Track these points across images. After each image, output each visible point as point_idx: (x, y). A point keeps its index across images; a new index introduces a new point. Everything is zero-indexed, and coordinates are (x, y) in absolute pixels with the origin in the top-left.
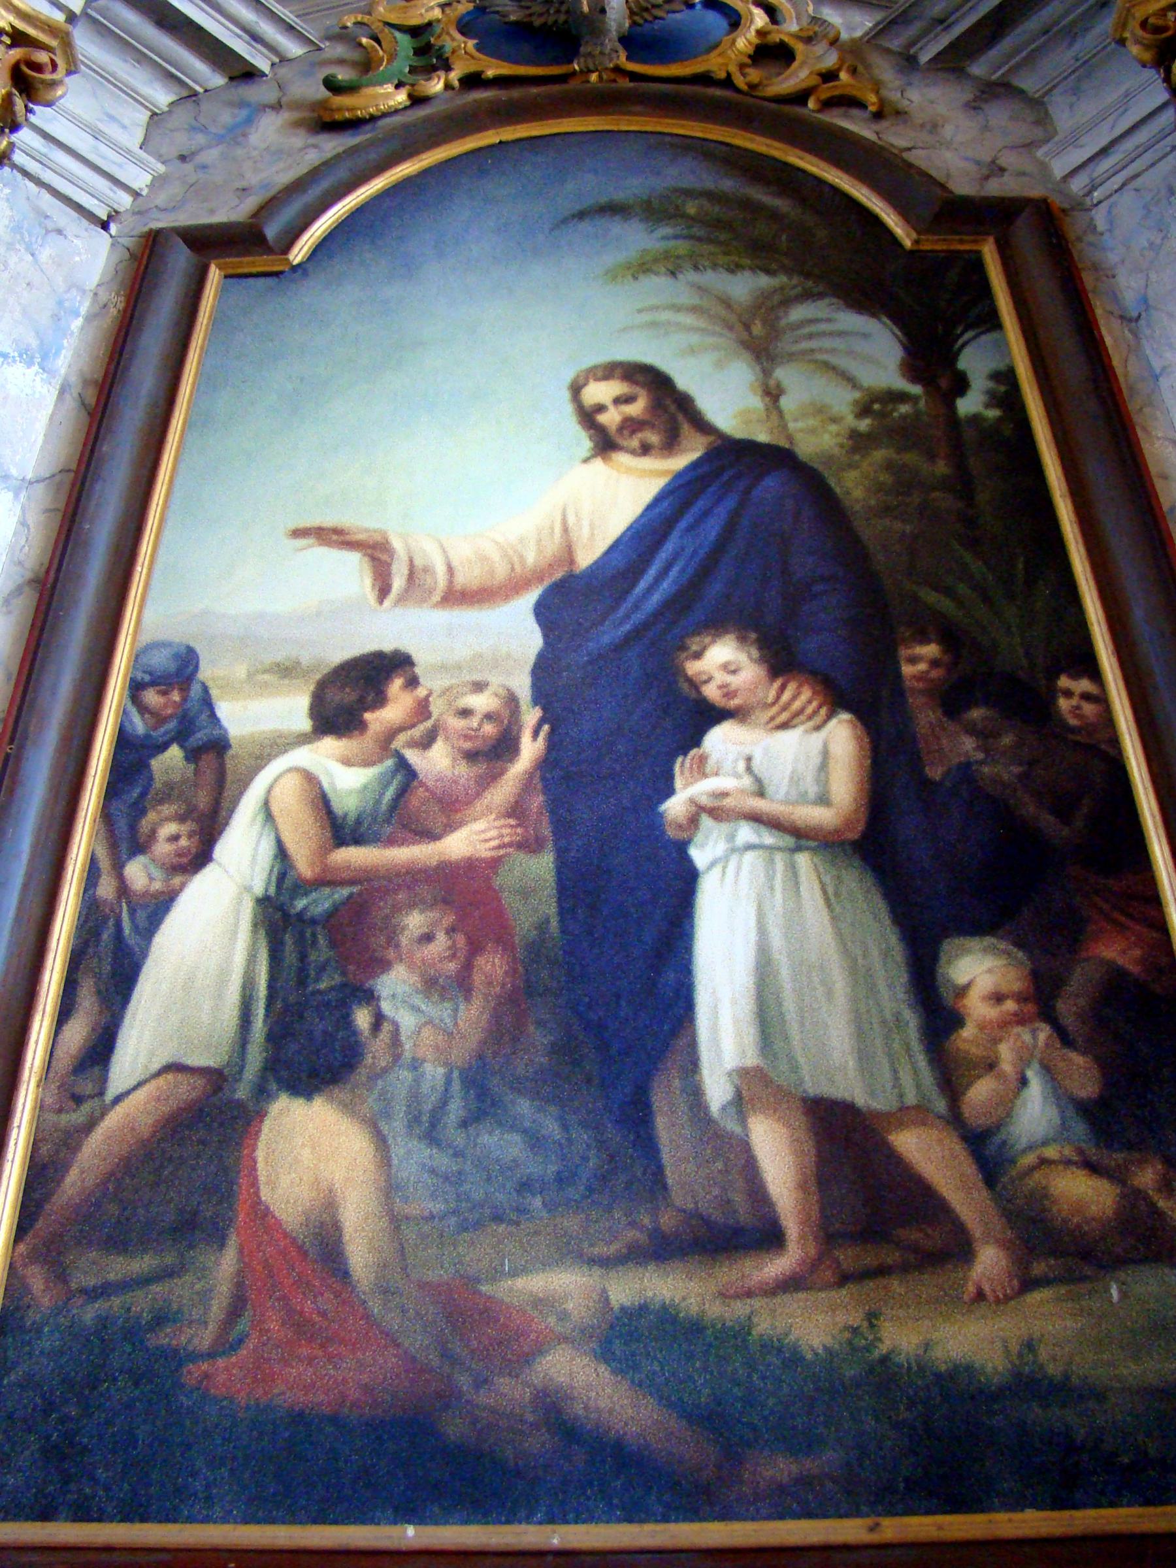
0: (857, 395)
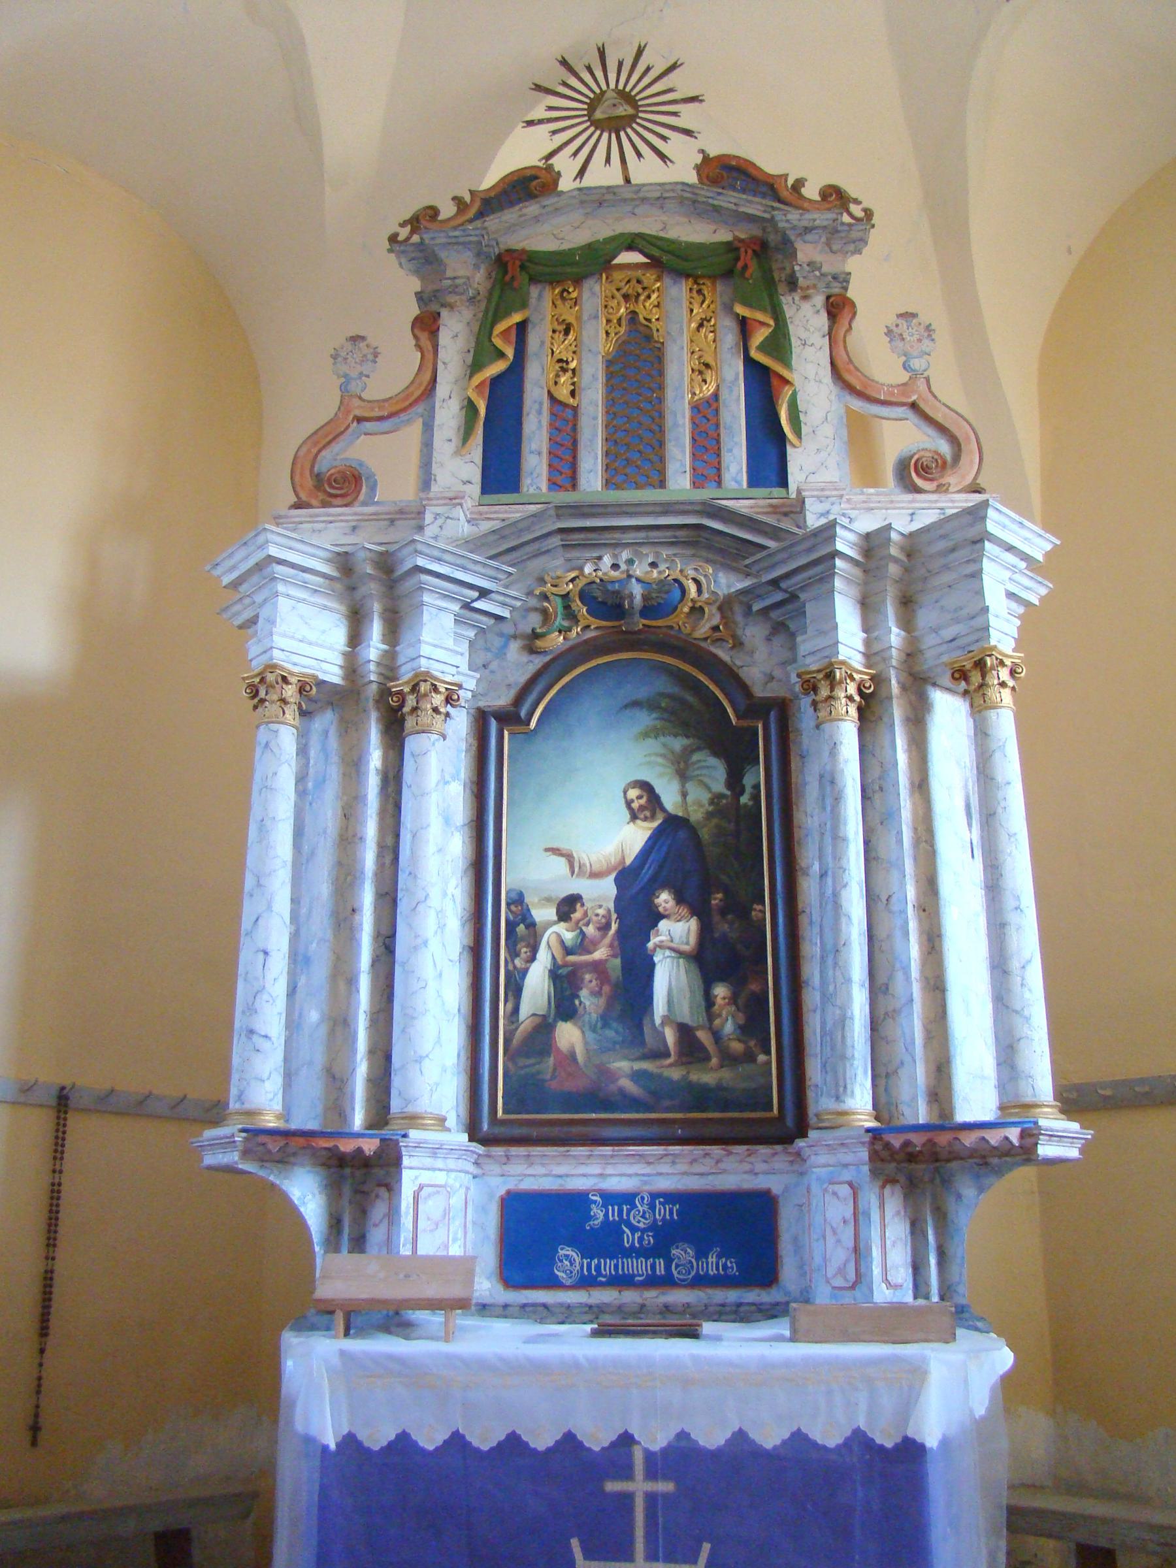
0: (710, 795)
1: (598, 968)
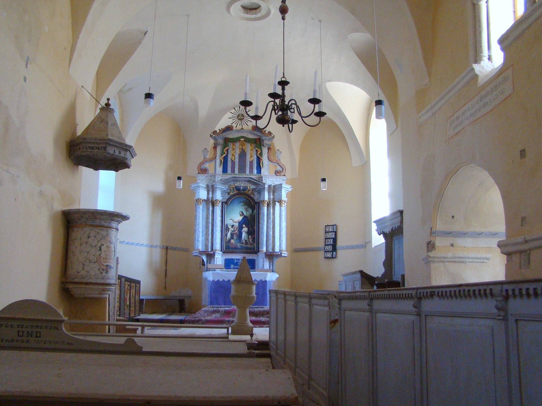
1: (236, 233)
